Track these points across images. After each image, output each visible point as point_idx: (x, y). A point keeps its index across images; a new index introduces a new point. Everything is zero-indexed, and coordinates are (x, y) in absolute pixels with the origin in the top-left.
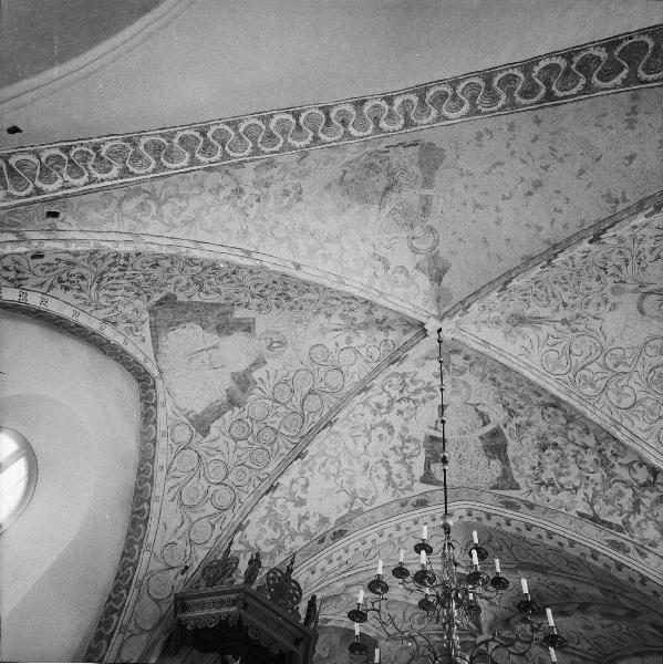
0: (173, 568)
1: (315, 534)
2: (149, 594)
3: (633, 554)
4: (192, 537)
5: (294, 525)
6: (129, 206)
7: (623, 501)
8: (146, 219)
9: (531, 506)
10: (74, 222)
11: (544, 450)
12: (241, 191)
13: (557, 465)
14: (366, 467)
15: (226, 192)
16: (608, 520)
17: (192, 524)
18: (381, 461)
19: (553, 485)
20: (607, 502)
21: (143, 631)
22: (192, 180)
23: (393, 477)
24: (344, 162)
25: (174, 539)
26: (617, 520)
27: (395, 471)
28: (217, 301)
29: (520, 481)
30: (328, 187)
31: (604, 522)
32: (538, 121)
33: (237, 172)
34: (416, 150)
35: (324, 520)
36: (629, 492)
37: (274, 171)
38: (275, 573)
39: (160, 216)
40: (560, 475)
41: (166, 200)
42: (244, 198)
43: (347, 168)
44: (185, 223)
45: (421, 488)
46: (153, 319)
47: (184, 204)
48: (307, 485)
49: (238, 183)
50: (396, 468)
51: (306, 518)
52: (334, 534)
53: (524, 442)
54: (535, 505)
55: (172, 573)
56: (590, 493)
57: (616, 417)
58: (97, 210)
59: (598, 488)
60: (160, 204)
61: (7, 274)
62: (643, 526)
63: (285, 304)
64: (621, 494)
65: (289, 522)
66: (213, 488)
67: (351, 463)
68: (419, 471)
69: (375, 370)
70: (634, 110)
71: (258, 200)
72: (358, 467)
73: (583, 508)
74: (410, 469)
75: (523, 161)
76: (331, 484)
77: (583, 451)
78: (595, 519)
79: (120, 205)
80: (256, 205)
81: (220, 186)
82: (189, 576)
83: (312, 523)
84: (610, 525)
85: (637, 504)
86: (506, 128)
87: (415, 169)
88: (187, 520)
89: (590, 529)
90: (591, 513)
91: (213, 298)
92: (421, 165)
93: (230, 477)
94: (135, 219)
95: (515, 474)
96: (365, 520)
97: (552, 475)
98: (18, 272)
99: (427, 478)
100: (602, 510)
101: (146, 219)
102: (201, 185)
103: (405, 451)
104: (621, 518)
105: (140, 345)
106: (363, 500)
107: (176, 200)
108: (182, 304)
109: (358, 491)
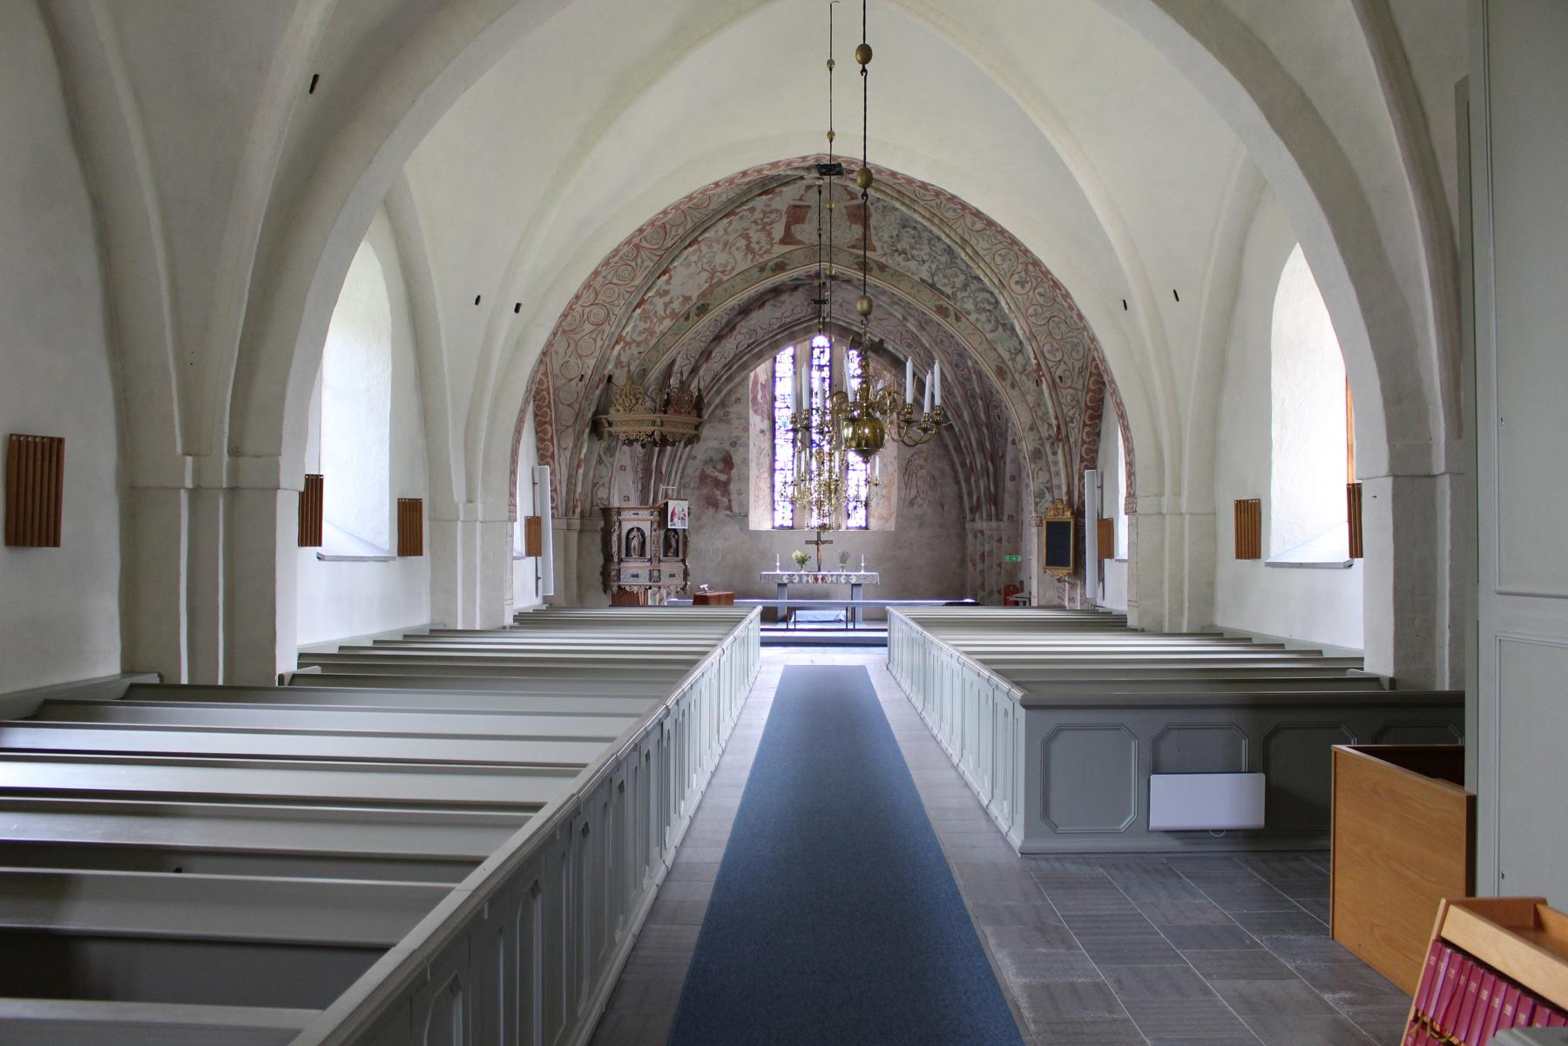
0: (571, 380)
1: (680, 312)
2: (562, 403)
3: (952, 319)
4: (580, 351)
5: (661, 312)
7: (956, 280)
9: (882, 267)
11: (904, 227)
13: (913, 241)
14: (725, 245)
16: (943, 289)
17: (577, 344)
18: (740, 236)
19: (906, 253)
20: (945, 276)
21: (568, 427)
23: (752, 245)
26: (948, 290)
27: (754, 240)
29: (876, 244)
31: (938, 290)
35: (687, 299)
36: (962, 277)
40: (913, 248)
45: (780, 250)
48: (671, 277)
50: (755, 236)
51: (671, 302)
52: (698, 308)
53: (887, 218)
54: (886, 266)
55: (573, 383)
56: (934, 267)
57: (966, 237)
59: (941, 266)
62: (966, 299)
64: (957, 276)
65: (656, 312)
66: (587, 310)
67: (710, 247)
68: (778, 231)
69: (744, 194)
72: (717, 247)
73: (925, 276)
74: (769, 234)
76: (693, 268)
77: (936, 240)
78: (933, 286)
83: (676, 305)
84: (942, 293)
85: (965, 286)
88: (572, 342)
89: (927, 294)
90: (930, 281)
93: (600, 297)
95: (874, 238)
96: (726, 290)
97: (908, 247)
99: (787, 239)
100: (940, 281)
103: (765, 220)
104: (952, 290)
106: (722, 272)
109: (717, 267)
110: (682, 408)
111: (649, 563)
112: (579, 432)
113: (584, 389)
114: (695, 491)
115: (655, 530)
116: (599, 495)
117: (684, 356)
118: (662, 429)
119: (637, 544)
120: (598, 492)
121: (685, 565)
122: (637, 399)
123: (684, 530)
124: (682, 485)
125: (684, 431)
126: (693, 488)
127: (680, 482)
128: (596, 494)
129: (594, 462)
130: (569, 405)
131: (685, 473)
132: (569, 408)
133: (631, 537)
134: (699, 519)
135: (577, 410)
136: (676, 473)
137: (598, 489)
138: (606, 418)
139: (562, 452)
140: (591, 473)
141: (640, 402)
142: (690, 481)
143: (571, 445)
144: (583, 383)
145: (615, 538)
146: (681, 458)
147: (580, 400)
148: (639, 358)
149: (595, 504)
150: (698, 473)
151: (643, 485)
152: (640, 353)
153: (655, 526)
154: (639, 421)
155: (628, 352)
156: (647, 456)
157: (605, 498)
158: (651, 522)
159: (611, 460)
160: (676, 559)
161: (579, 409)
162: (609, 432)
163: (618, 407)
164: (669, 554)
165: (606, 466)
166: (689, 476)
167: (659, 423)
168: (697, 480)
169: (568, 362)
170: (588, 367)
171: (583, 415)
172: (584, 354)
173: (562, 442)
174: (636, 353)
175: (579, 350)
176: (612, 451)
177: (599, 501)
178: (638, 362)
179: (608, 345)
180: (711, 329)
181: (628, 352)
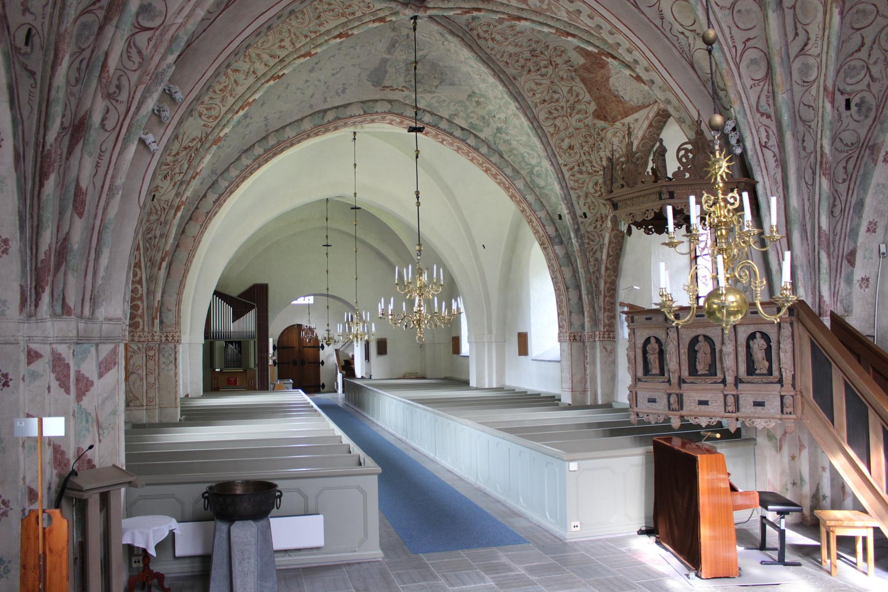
6: (542, 183)
8: (543, 170)
10: (560, 207)
12: (498, 129)
15: (504, 136)
22: (512, 157)
24: (433, 95)
28: (582, 85)
30: (452, 84)
32: (311, 106)
33: (491, 139)
34: (387, 83)
37: (474, 121)
39: (539, 164)
41: (530, 164)
42: (500, 125)
43: (434, 89)
44: (533, 150)
46: (619, 117)
47: (525, 154)
49: (495, 134)
58: (550, 198)
60: (533, 167)
61: (599, 226)
63: (539, 48)
70: (266, 125)
71: (494, 116)
75: (319, 81)
79: (543, 188)
80: (498, 116)
81: (504, 142)
86: (329, 99)
87: (391, 70)
91: (579, 87)
92: (386, 72)
94: (546, 177)
98: (597, 221)
101: (543, 170)
102: (511, 151)
105: (640, 122)
107: (526, 159)
108: (598, 104)
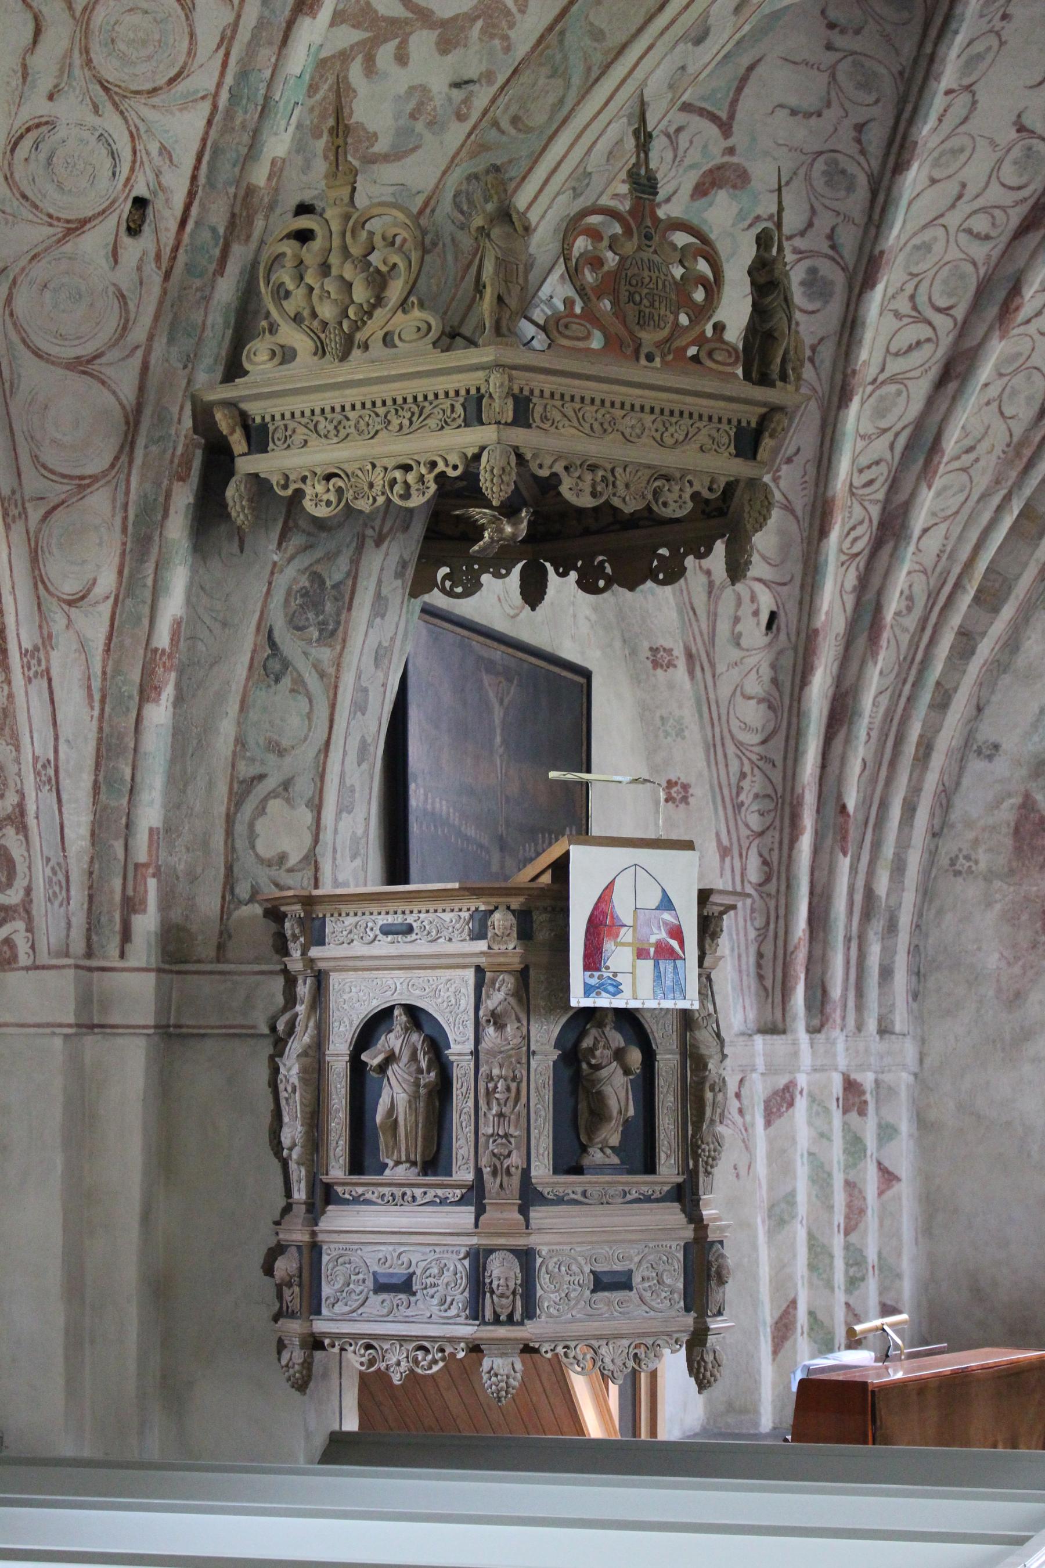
2: (37, 353)
4: (110, 70)
25: (37, 106)
38: (595, 234)
82: (168, 238)
110: (643, 320)
111: (465, 1216)
112: (146, 509)
113: (156, 279)
114: (997, 884)
115: (497, 1020)
116: (261, 848)
117: (903, 305)
118: (519, 436)
119: (402, 1099)
120: (259, 826)
121: (695, 1217)
122: (379, 281)
123: (686, 1019)
124: (944, 861)
125: (669, 459)
126: (989, 877)
127: (932, 855)
128: (252, 837)
129: (241, 671)
130: (81, 366)
131: (955, 816)
132: (76, 382)
133: (372, 1058)
134: (1016, 999)
135: (128, 391)
136: (910, 809)
137: (261, 810)
138: (231, 405)
139: (58, 621)
140: (227, 728)
141: (395, 291)
142: (976, 842)
143: (107, 581)
144: (146, 241)
145: (291, 1069)
146: (925, 748)
147: (138, 334)
148: (461, 117)
149: (243, 890)
150: (1007, 814)
151: (765, 863)
152: (457, 85)
153: (496, 998)
154: (398, 405)
155: (399, 80)
156: (779, 741)
157: (293, 860)
158: (479, 970)
159: (325, 654)
160: (642, 1184)
161: (142, 389)
162: (259, 484)
163: (291, 336)
164: (596, 1156)
165: (299, 686)
166: (969, 824)
167: (502, 408)
168: (1009, 842)
169: (50, 124)
170: (163, 150)
171: (161, 418)
172: (142, 75)
173: (54, 568)
174: (438, 85)
175: (98, 56)
176: (329, 607)
177: (263, 876)
178: (456, 134)
179: (261, 25)
180: (1009, 174)
181: (399, 80)
